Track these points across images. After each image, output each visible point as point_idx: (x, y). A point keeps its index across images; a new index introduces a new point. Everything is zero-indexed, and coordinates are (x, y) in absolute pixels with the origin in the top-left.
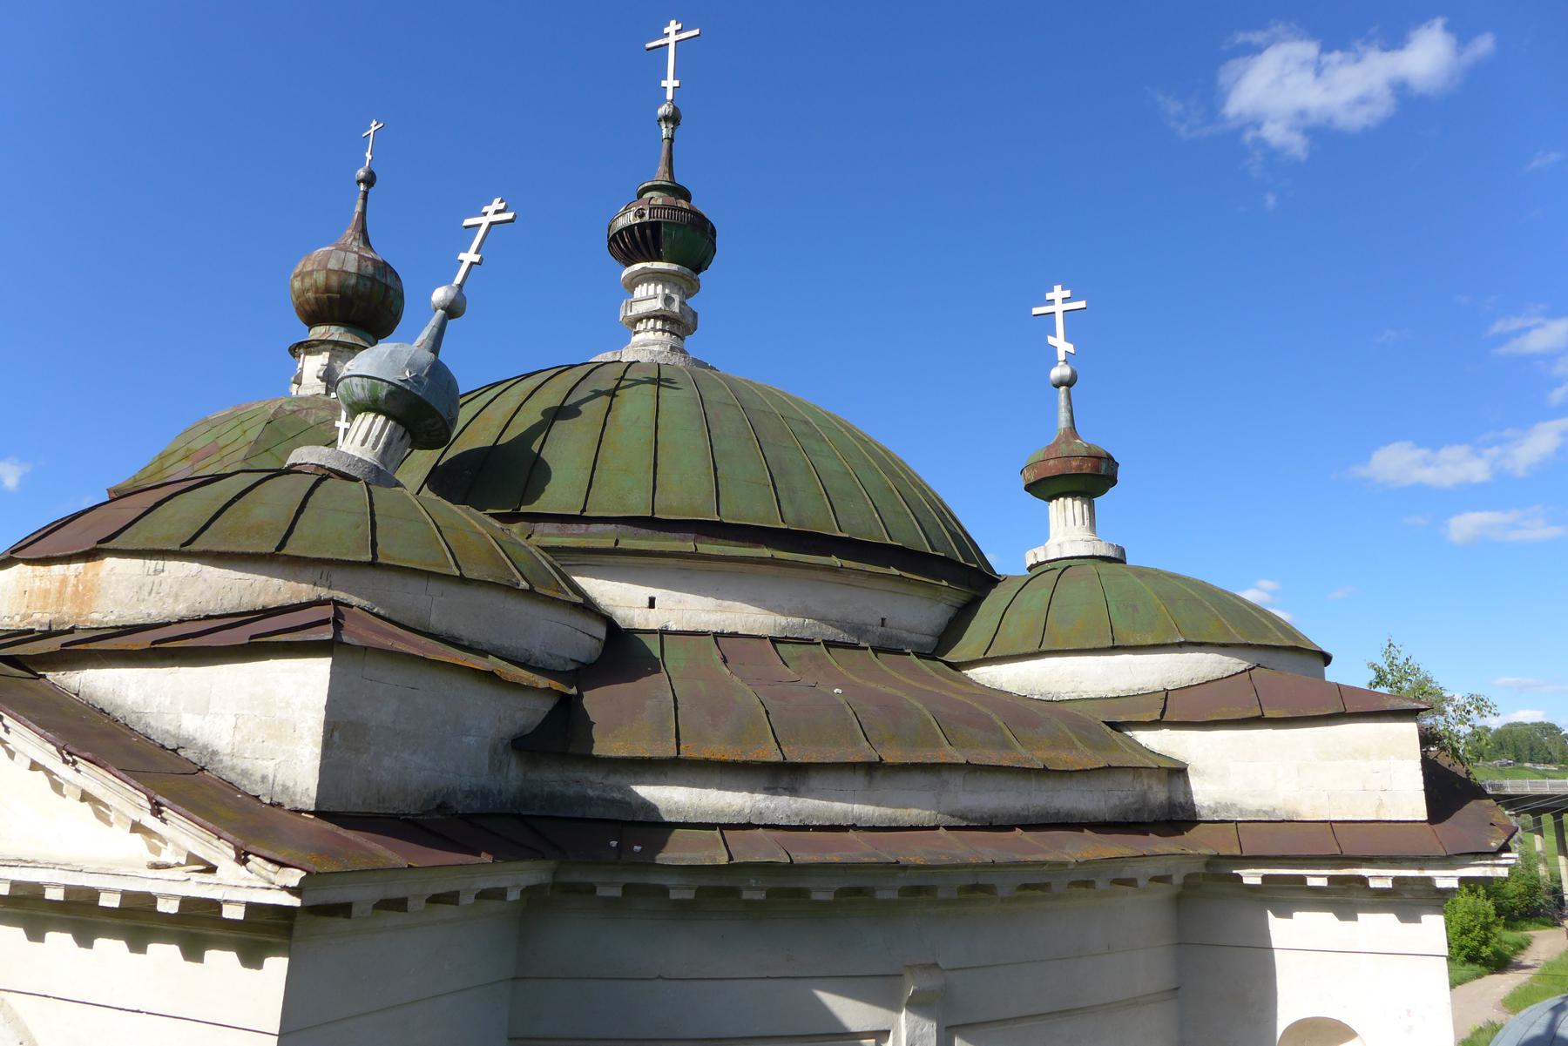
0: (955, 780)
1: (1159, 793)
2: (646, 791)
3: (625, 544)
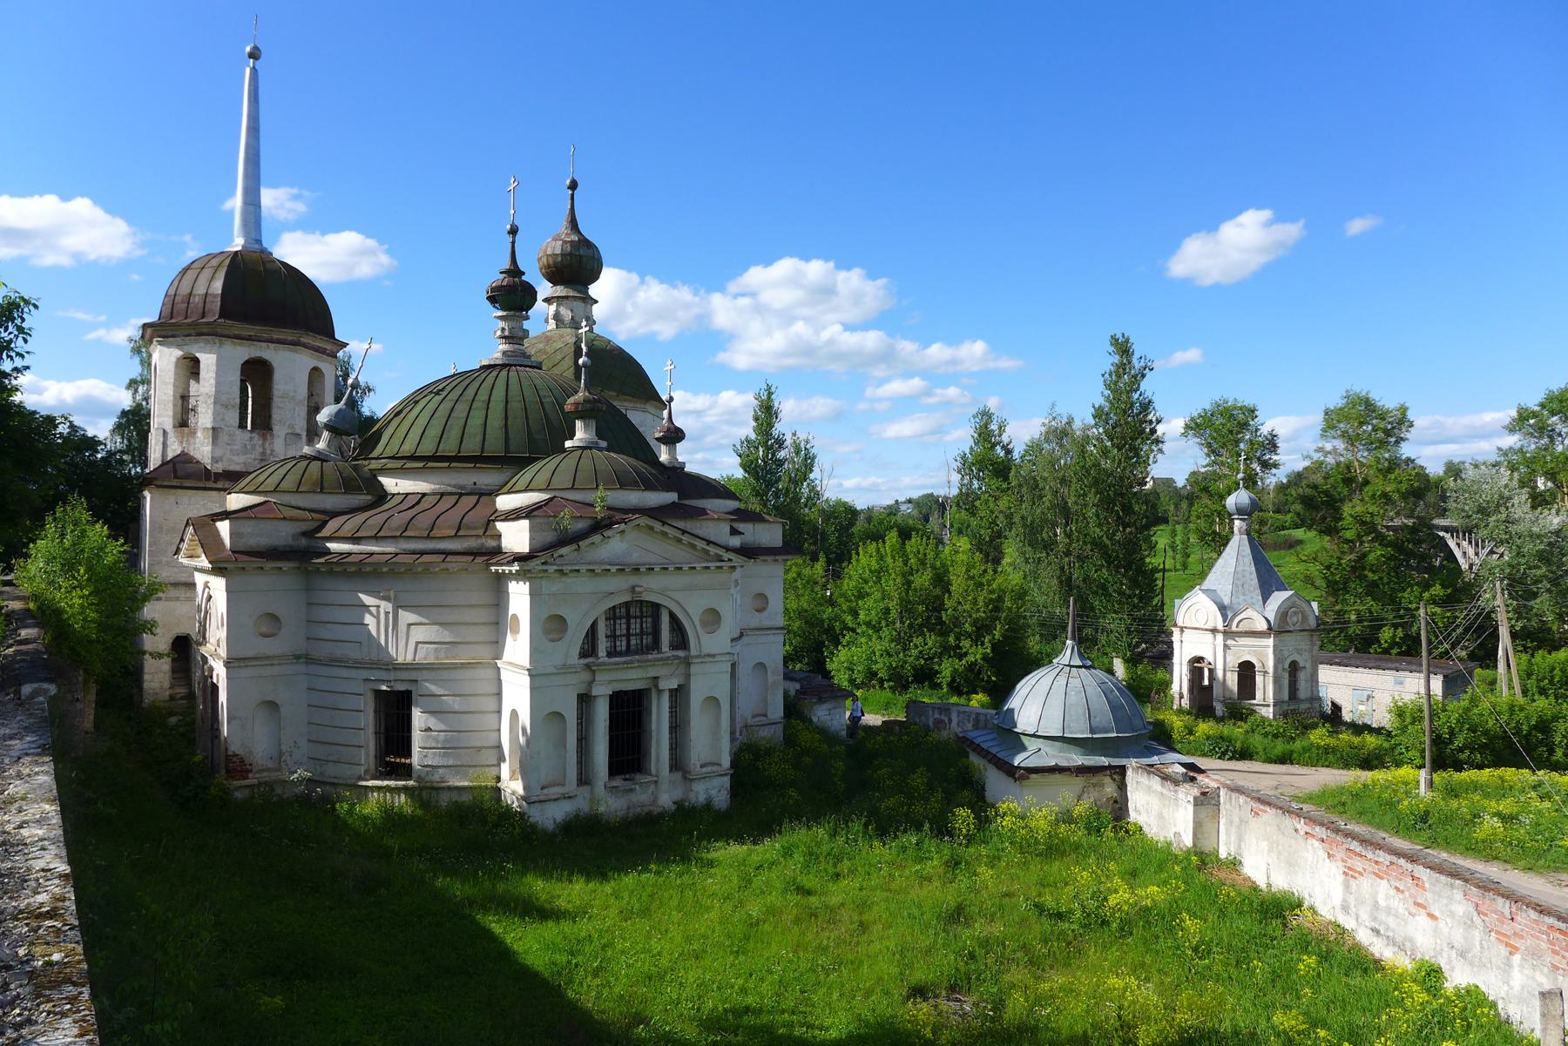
0: (402, 541)
1: (491, 543)
2: (328, 545)
3: (389, 466)
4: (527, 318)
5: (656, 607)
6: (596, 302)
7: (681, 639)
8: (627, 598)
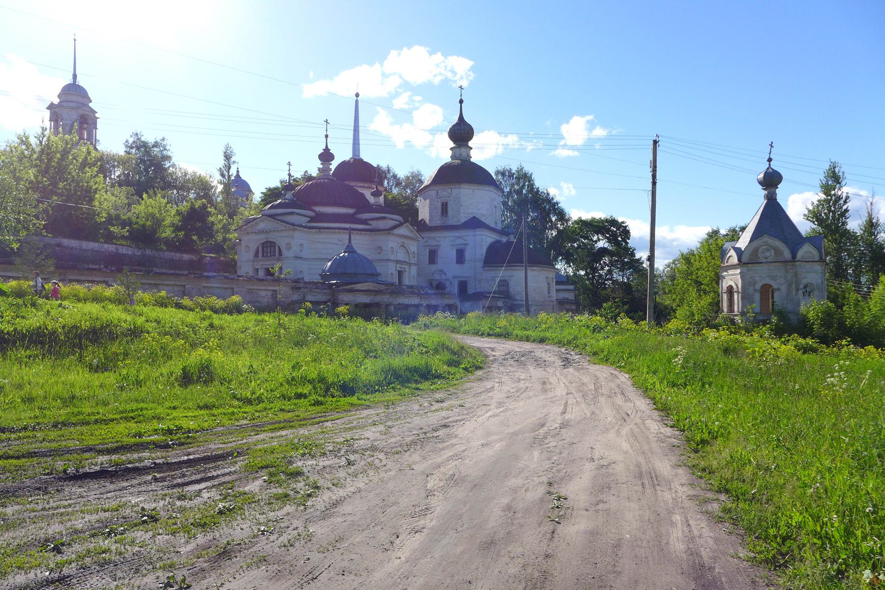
4: (331, 164)
5: (275, 243)
6: (472, 148)
7: (280, 254)
8: (265, 240)
